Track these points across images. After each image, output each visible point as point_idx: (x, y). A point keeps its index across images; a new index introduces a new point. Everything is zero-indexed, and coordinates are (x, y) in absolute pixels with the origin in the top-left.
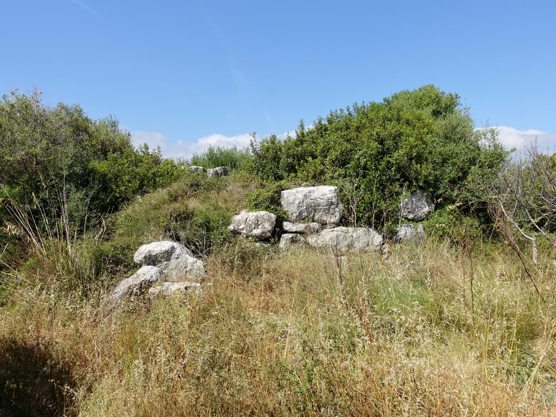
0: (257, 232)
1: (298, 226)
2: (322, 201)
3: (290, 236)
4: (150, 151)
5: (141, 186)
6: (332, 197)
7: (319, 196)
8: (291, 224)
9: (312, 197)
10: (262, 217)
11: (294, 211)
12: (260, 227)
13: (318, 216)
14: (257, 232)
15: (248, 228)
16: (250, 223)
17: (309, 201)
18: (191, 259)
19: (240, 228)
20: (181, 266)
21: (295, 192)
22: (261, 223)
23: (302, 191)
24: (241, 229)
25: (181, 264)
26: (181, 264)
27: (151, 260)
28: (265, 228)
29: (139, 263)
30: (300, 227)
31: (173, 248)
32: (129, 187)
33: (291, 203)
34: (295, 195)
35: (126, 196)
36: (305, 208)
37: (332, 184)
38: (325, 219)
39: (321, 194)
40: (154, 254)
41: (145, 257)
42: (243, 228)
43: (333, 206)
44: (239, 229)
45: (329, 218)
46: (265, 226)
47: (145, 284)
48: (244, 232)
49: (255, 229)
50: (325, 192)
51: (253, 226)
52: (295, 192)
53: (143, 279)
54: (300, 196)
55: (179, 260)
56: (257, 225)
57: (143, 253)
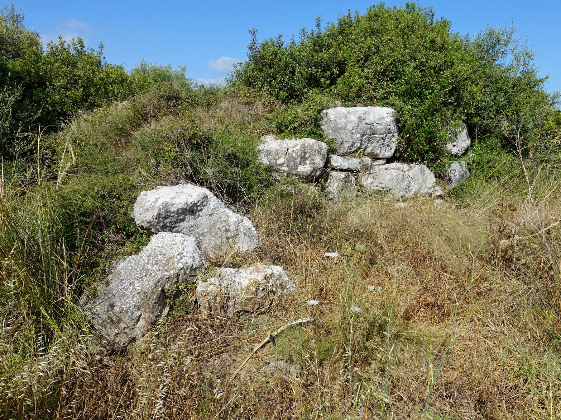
0: (305, 169)
1: (350, 161)
2: (379, 127)
3: (343, 175)
4: (87, 50)
5: (86, 95)
6: (390, 121)
7: (375, 119)
8: (342, 158)
9: (368, 121)
10: (311, 147)
11: (346, 139)
12: (308, 162)
13: (371, 148)
14: (305, 170)
15: (292, 164)
16: (294, 155)
17: (363, 125)
18: (233, 217)
19: (278, 162)
20: (219, 229)
21: (346, 113)
22: (309, 156)
23: (356, 112)
24: (280, 165)
25: (218, 226)
26: (218, 226)
27: (169, 221)
28: (315, 163)
29: (146, 225)
30: (353, 163)
31: (205, 197)
32: (67, 97)
33: (340, 129)
34: (346, 117)
35: (62, 110)
36: (359, 135)
37: (386, 104)
38: (378, 152)
39: (377, 117)
40: (174, 209)
41: (159, 215)
42: (283, 164)
43: (391, 135)
44: (277, 165)
45: (384, 151)
46: (315, 161)
47: (185, 274)
48: (284, 168)
49: (300, 164)
50: (382, 115)
51: (298, 160)
52: (346, 113)
53: (180, 266)
54: (354, 119)
55: (215, 218)
56: (304, 159)
57: (153, 207)
